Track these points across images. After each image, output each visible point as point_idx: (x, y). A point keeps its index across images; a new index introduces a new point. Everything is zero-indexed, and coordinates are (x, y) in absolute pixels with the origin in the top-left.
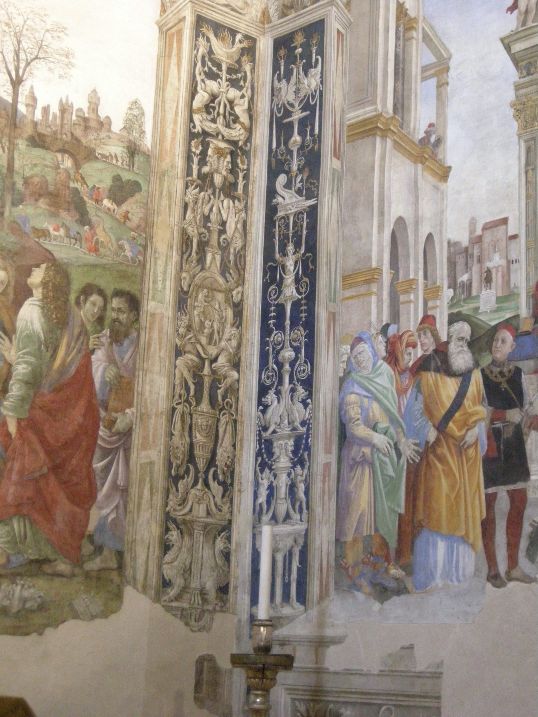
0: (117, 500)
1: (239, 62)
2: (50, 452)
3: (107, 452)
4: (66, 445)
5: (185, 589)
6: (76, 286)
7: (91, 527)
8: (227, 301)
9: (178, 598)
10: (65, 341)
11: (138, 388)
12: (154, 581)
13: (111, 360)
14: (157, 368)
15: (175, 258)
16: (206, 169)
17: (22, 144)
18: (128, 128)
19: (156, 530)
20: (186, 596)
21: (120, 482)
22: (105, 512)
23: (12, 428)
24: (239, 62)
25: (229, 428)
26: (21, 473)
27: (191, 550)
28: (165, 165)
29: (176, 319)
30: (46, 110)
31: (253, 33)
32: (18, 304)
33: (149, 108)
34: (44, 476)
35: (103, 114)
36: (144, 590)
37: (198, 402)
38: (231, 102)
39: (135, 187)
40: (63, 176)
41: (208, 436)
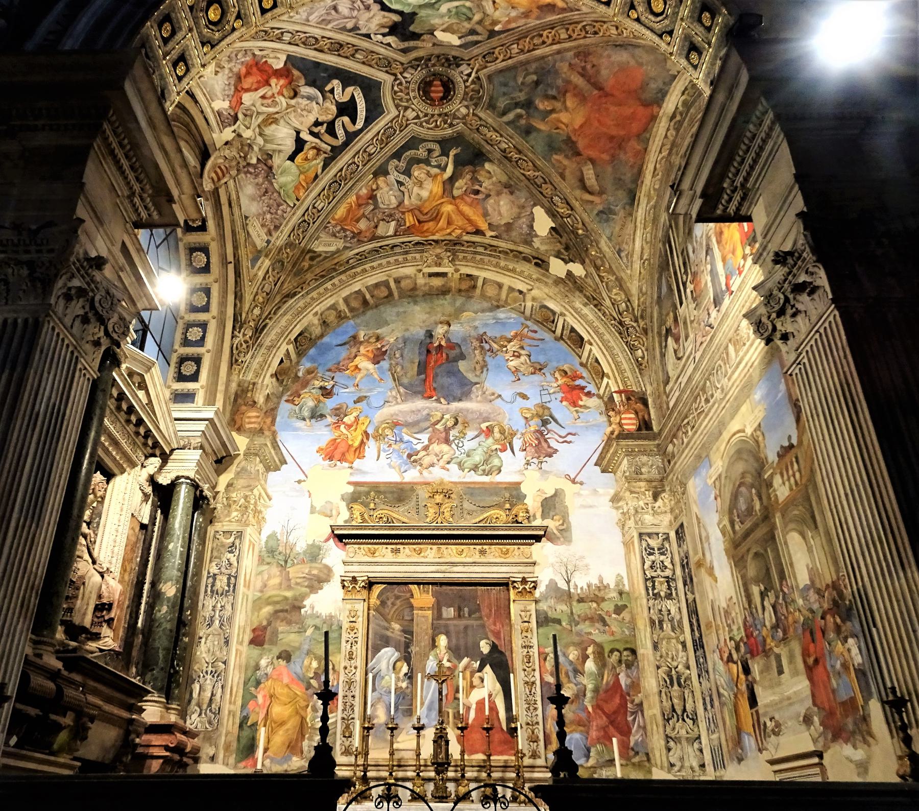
0: (641, 732)
1: (663, 545)
2: (608, 716)
3: (633, 713)
4: (615, 712)
5: (682, 767)
6: (607, 650)
7: (632, 744)
8: (678, 642)
9: (679, 771)
10: (606, 672)
11: (642, 684)
12: (666, 764)
13: (628, 676)
14: (649, 675)
15: (649, 629)
16: (656, 591)
17: (575, 603)
18: (617, 585)
19: (663, 743)
20: (684, 770)
21: (641, 724)
22: (637, 737)
23: (590, 709)
24: (663, 545)
25: (690, 695)
26: (597, 726)
27: (682, 749)
28: (636, 595)
29: (654, 655)
30: (582, 588)
31: (667, 531)
32: (584, 662)
33: (624, 575)
34: (607, 726)
35: (605, 583)
36: (662, 768)
37: (672, 686)
38: (662, 562)
39: (625, 606)
40: (593, 611)
41: (680, 699)
